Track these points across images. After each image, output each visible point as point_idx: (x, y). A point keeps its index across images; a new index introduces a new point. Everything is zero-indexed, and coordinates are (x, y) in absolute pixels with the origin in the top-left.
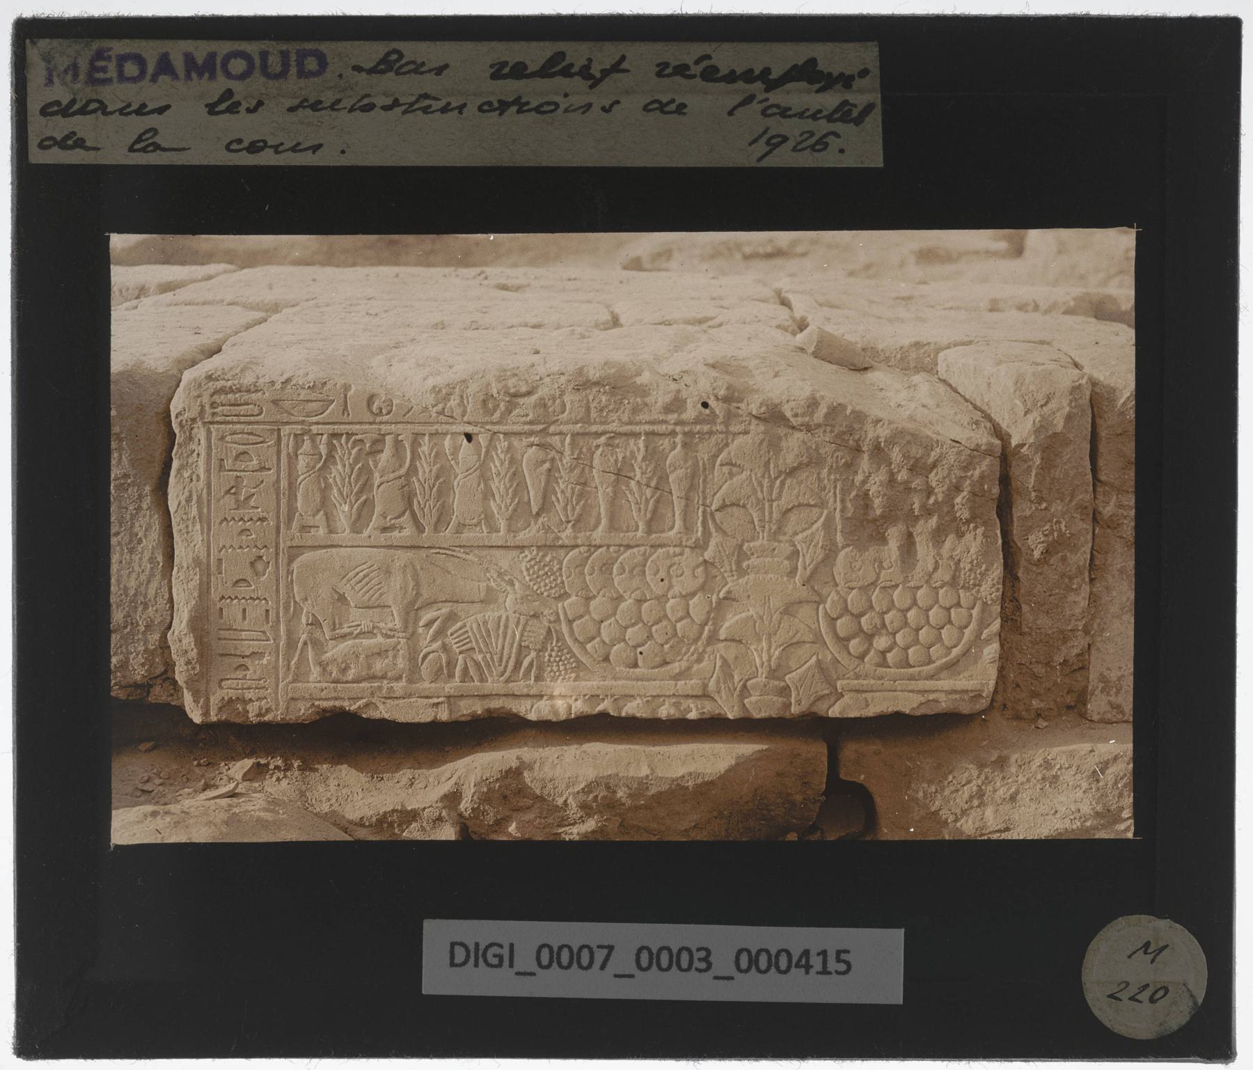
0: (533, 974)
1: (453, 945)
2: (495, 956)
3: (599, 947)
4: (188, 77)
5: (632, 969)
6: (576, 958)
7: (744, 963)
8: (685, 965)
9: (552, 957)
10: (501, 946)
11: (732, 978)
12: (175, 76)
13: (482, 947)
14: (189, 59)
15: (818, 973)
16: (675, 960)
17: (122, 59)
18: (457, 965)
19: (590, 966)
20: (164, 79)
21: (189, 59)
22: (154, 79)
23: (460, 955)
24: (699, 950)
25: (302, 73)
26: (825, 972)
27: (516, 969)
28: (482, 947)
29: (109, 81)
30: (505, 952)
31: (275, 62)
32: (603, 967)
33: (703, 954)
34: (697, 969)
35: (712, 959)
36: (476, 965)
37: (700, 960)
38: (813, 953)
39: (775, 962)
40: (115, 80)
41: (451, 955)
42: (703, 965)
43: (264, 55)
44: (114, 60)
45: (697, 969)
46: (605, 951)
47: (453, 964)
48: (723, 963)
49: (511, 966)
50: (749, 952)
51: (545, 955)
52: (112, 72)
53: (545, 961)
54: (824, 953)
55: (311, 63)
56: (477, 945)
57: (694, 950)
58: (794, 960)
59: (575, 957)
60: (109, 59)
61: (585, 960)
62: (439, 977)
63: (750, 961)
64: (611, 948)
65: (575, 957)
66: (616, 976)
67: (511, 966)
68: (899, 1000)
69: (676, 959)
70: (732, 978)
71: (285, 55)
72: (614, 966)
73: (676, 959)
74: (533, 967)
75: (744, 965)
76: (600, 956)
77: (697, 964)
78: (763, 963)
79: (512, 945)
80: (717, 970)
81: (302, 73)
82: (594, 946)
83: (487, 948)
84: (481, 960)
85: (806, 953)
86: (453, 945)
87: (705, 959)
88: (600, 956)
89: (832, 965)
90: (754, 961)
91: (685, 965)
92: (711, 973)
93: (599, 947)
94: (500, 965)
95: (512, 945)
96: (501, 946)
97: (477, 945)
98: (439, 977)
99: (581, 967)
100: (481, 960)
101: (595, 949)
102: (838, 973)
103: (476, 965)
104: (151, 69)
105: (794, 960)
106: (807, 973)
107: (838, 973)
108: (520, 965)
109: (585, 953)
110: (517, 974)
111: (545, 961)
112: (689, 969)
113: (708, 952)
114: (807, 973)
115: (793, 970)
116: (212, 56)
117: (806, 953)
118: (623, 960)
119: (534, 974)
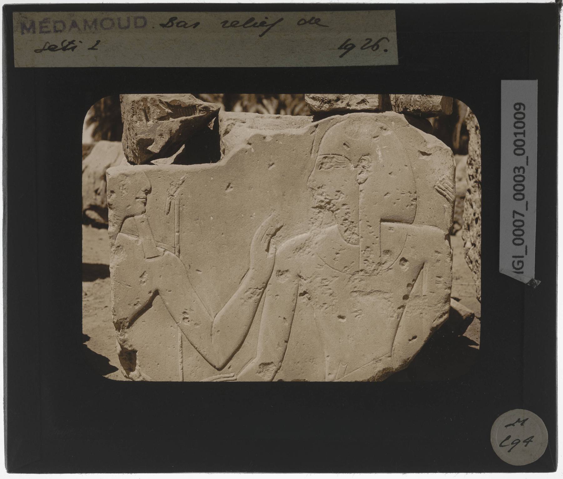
0: (526, 247)
3: (514, 217)
5: (524, 202)
6: (518, 227)
7: (521, 152)
9: (518, 239)
10: (514, 262)
11: (527, 157)
13: (515, 270)
16: (519, 183)
19: (522, 221)
24: (515, 173)
27: (524, 254)
32: (523, 215)
33: (517, 170)
34: (524, 173)
37: (519, 172)
42: (521, 170)
45: (524, 173)
48: (520, 161)
49: (523, 257)
51: (517, 242)
53: (520, 242)
57: (514, 175)
59: (519, 228)
61: (520, 223)
64: (515, 212)
66: (527, 209)
67: (523, 257)
68: (536, 82)
70: (527, 157)
72: (523, 211)
73: (519, 183)
74: (523, 247)
76: (517, 217)
77: (521, 173)
79: (513, 257)
80: (524, 165)
82: (514, 220)
83: (514, 268)
84: (521, 271)
87: (519, 169)
88: (517, 217)
92: (526, 167)
93: (514, 217)
94: (522, 262)
95: (513, 257)
96: (514, 262)
100: (521, 271)
103: (522, 273)
110: (526, 254)
111: (520, 242)
112: (523, 176)
113: (516, 168)
118: (520, 206)
119: (526, 247)
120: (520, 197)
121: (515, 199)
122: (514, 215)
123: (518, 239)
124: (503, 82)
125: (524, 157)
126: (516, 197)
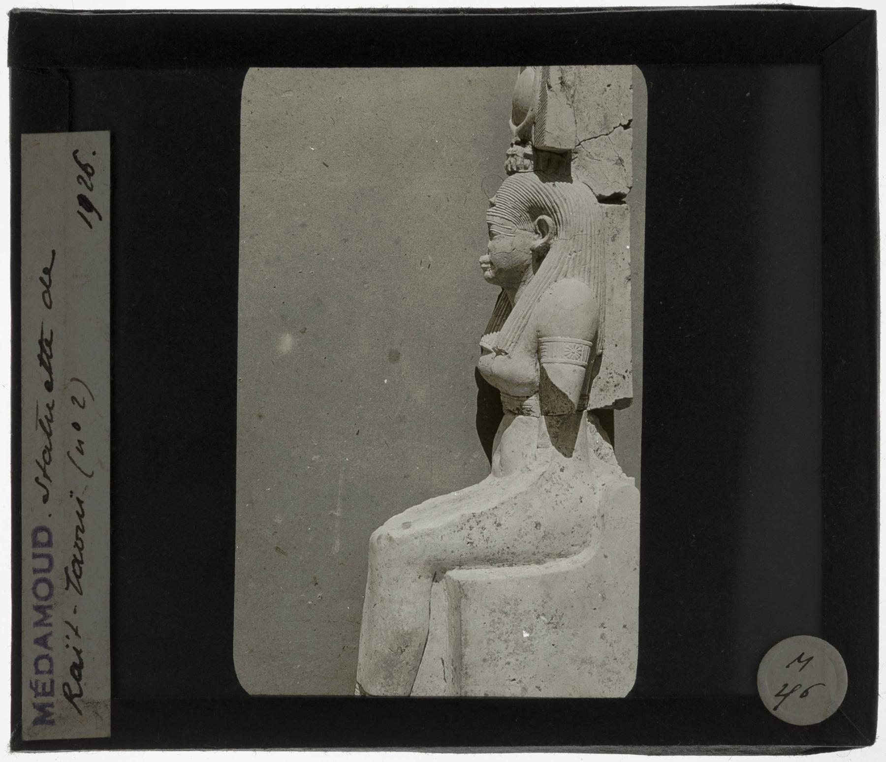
4: (50, 625)
12: (50, 634)
14: (38, 624)
17: (38, 672)
20: (51, 642)
21: (38, 624)
22: (50, 649)
25: (49, 544)
29: (52, 682)
31: (43, 563)
40: (51, 676)
43: (35, 571)
44: (38, 677)
52: (45, 678)
55: (43, 537)
60: (37, 682)
71: (35, 556)
81: (49, 544)
104: (44, 651)
116: (38, 608)
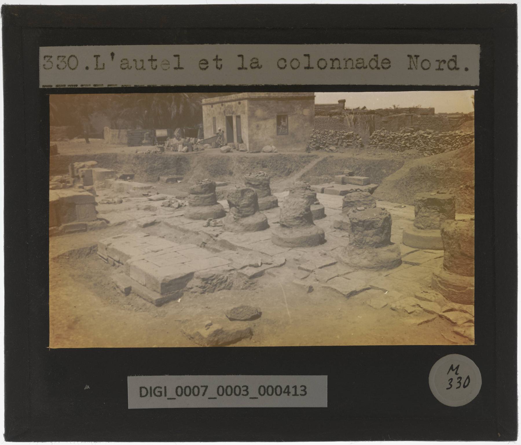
0: (175, 399)
1: (141, 388)
2: (158, 392)
3: (202, 386)
5: (216, 395)
6: (192, 391)
8: (237, 393)
10: (161, 388)
13: (153, 389)
15: (293, 395)
16: (233, 391)
18: (144, 396)
23: (144, 392)
26: (296, 394)
27: (167, 397)
28: (153, 389)
30: (163, 390)
32: (203, 395)
33: (245, 388)
34: (243, 395)
35: (248, 390)
36: (151, 396)
38: (291, 388)
39: (275, 391)
41: (141, 392)
42: (245, 393)
45: (243, 395)
46: (204, 388)
47: (141, 396)
48: (253, 392)
49: (165, 395)
50: (264, 386)
51: (179, 390)
53: (179, 393)
54: (295, 387)
56: (151, 388)
57: (241, 387)
58: (283, 390)
59: (192, 391)
61: (196, 393)
62: (135, 402)
63: (264, 391)
65: (192, 391)
66: (209, 398)
67: (165, 395)
69: (234, 391)
72: (208, 394)
73: (234, 391)
74: (175, 396)
75: (262, 393)
76: (202, 390)
77: (242, 392)
78: (270, 391)
79: (165, 387)
85: (288, 387)
86: (141, 388)
87: (246, 390)
88: (202, 390)
89: (299, 392)
90: (266, 391)
91: (237, 393)
93: (202, 386)
94: (161, 395)
95: (165, 387)
96: (161, 388)
97: (151, 388)
98: (135, 402)
99: (194, 395)
101: (200, 387)
102: (301, 395)
103: (151, 396)
105: (283, 390)
106: (288, 395)
107: (301, 395)
108: (169, 395)
109: (196, 389)
110: (168, 399)
111: (179, 393)
113: (247, 387)
114: (288, 395)
115: (283, 394)
117: (288, 387)
118: (212, 392)
119: (175, 399)
120: (221, 392)
121: (219, 387)
122: (204, 386)
123: (181, 391)
124: (327, 376)
125: (257, 395)
126: (221, 389)
